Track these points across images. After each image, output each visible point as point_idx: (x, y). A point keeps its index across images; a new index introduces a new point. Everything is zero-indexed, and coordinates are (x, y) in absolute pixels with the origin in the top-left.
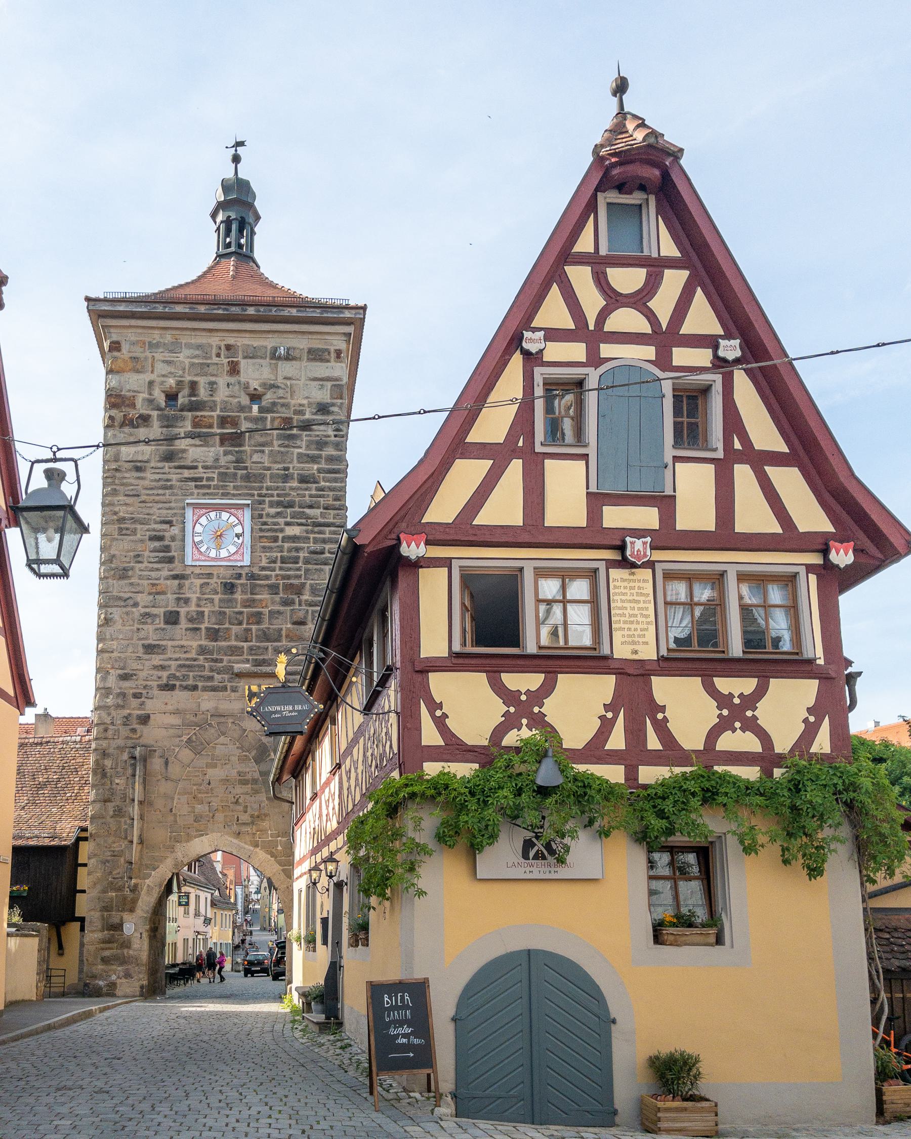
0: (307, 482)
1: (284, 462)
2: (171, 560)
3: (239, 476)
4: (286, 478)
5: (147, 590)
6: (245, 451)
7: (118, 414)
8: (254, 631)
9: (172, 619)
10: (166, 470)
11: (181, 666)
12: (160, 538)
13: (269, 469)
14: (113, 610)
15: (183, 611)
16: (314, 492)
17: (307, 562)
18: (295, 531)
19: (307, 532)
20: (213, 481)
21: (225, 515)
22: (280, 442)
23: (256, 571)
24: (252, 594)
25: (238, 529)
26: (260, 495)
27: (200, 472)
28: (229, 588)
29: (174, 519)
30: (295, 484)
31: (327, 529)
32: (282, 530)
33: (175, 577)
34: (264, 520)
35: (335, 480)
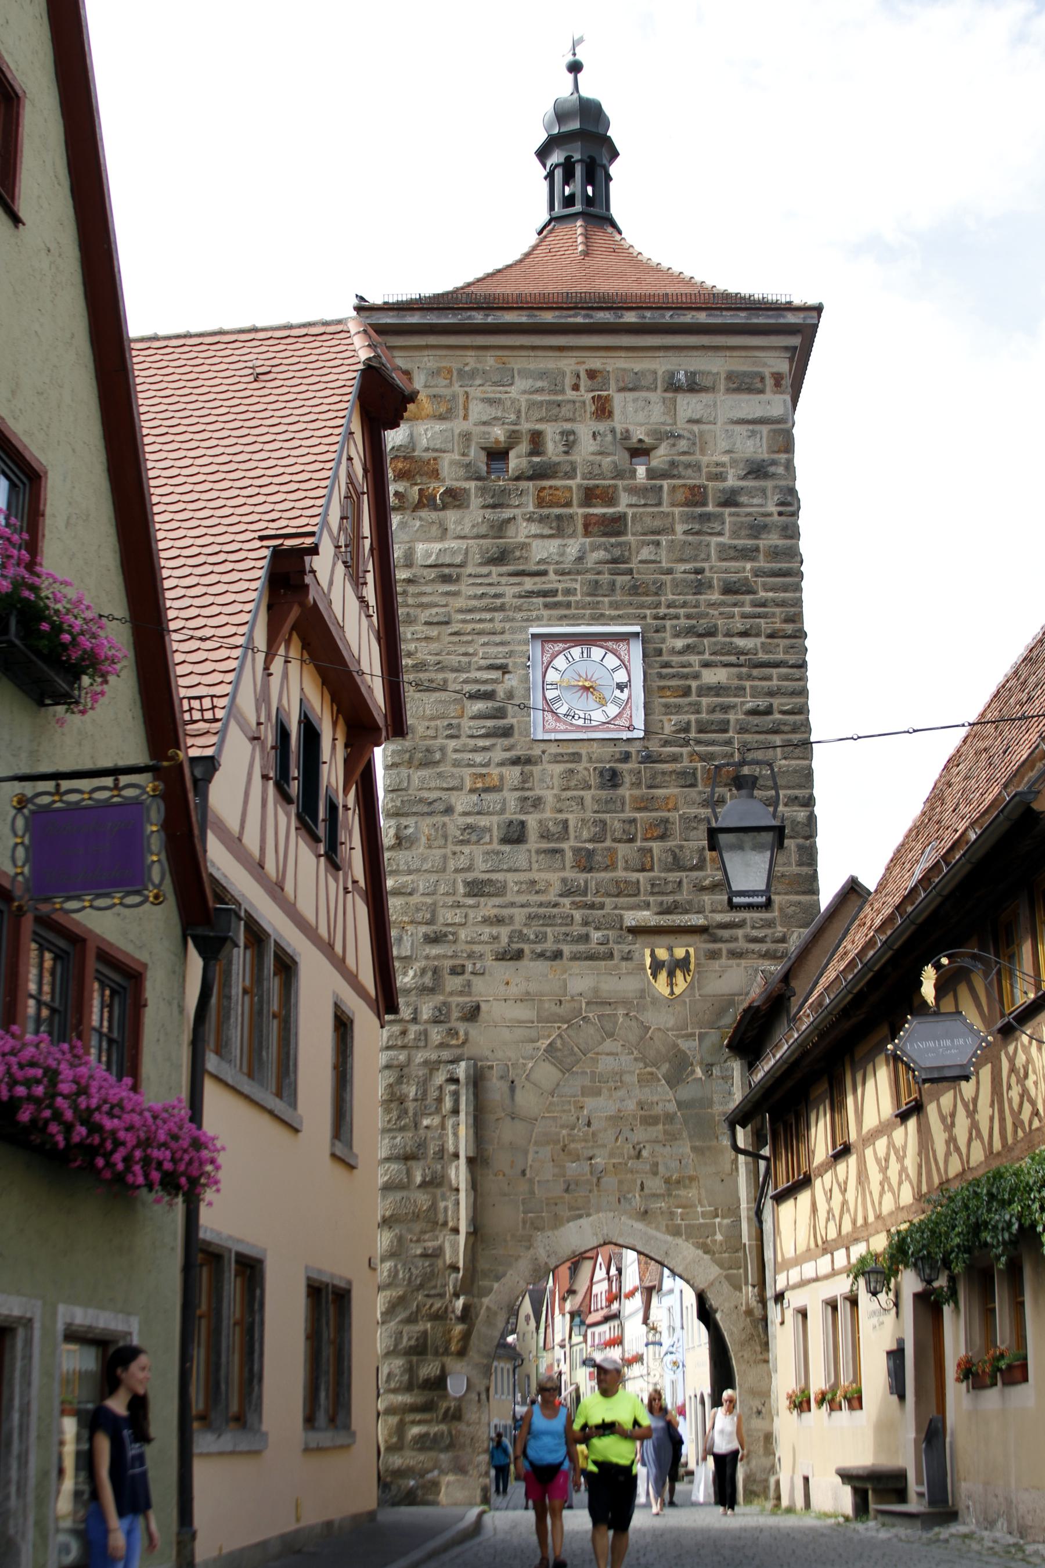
0: (736, 592)
1: (695, 560)
2: (507, 732)
3: (618, 585)
4: (700, 587)
5: (468, 784)
6: (628, 544)
8: (655, 852)
9: (515, 835)
10: (494, 578)
11: (530, 917)
12: (489, 696)
13: (669, 572)
14: (410, 821)
15: (532, 821)
16: (748, 609)
17: (743, 730)
19: (740, 677)
20: (575, 595)
21: (597, 652)
22: (686, 527)
23: (654, 747)
24: (650, 787)
25: (621, 676)
26: (656, 617)
27: (552, 581)
28: (612, 779)
29: (510, 661)
30: (715, 596)
31: (774, 672)
32: (697, 676)
33: (516, 762)
34: (665, 658)
35: (785, 589)
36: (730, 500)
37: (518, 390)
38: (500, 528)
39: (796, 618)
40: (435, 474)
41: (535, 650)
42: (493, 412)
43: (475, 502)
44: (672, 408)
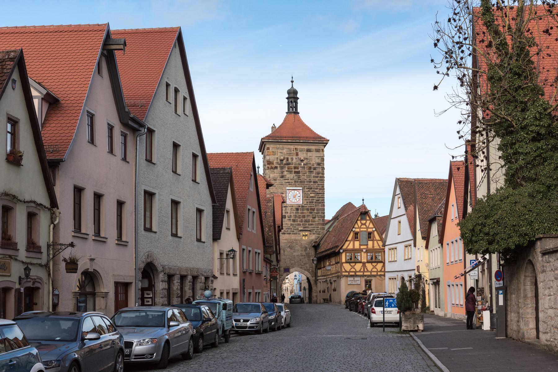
4: (310, 182)
7: (270, 166)
15: (287, 215)
18: (312, 195)
21: (296, 191)
27: (290, 181)
28: (297, 209)
36: (315, 169)
37: (285, 151)
38: (282, 172)
39: (323, 187)
40: (273, 164)
41: (287, 191)
42: (281, 154)
43: (279, 168)
44: (307, 155)
